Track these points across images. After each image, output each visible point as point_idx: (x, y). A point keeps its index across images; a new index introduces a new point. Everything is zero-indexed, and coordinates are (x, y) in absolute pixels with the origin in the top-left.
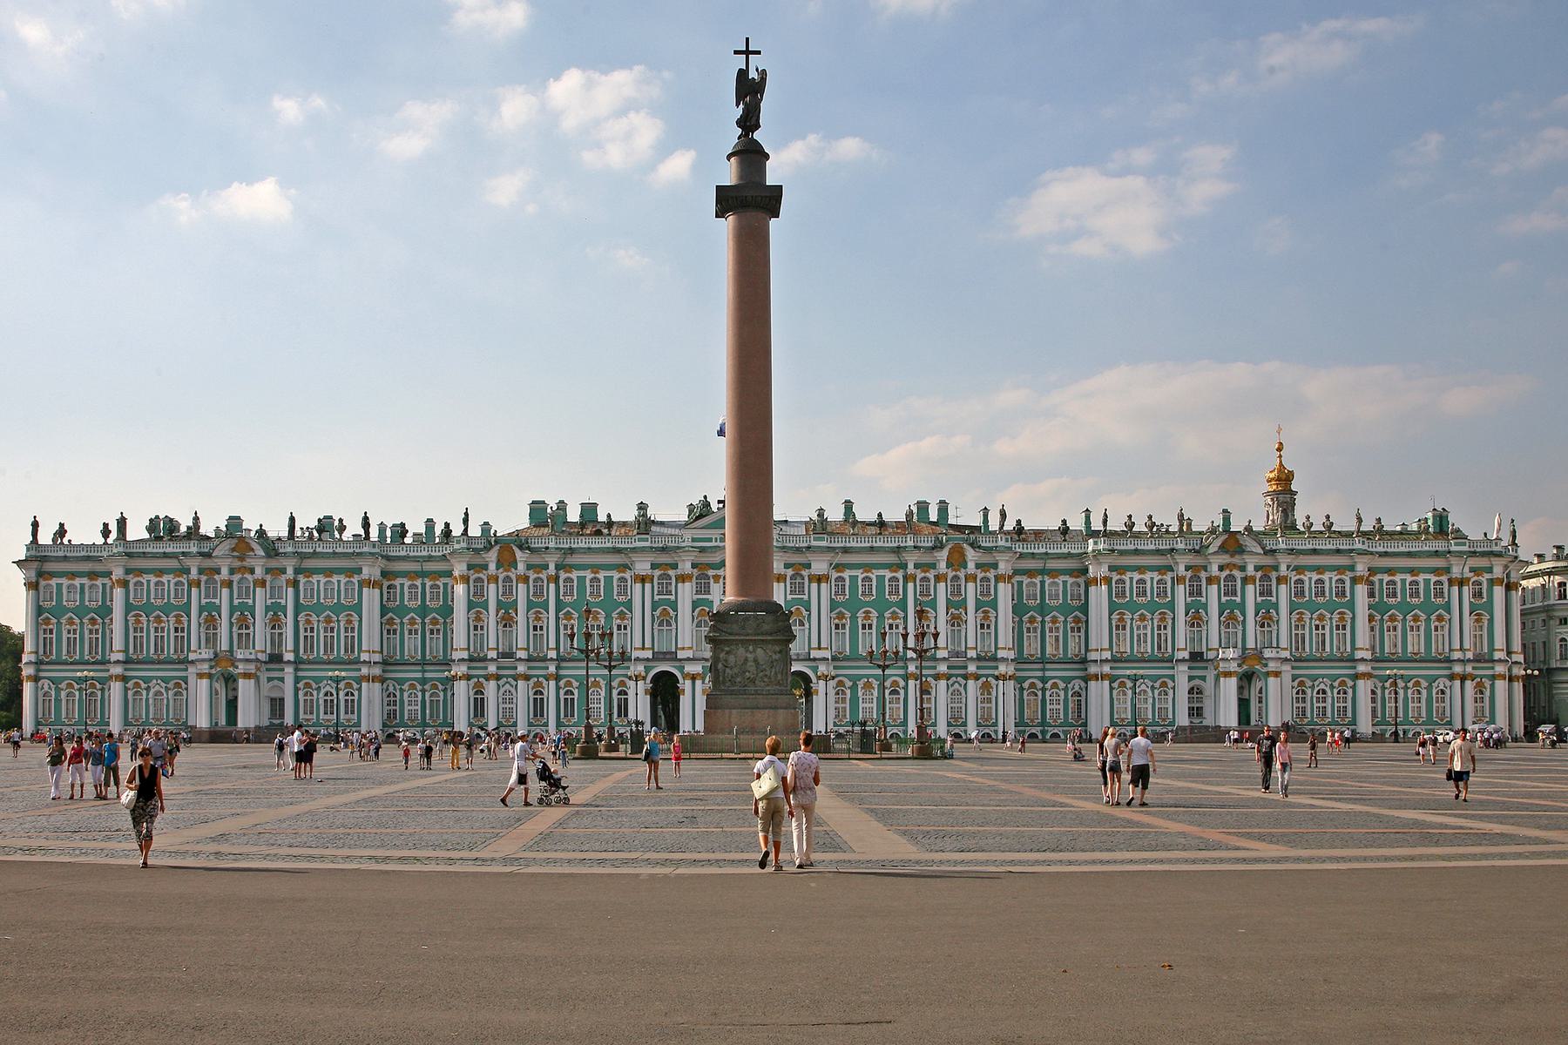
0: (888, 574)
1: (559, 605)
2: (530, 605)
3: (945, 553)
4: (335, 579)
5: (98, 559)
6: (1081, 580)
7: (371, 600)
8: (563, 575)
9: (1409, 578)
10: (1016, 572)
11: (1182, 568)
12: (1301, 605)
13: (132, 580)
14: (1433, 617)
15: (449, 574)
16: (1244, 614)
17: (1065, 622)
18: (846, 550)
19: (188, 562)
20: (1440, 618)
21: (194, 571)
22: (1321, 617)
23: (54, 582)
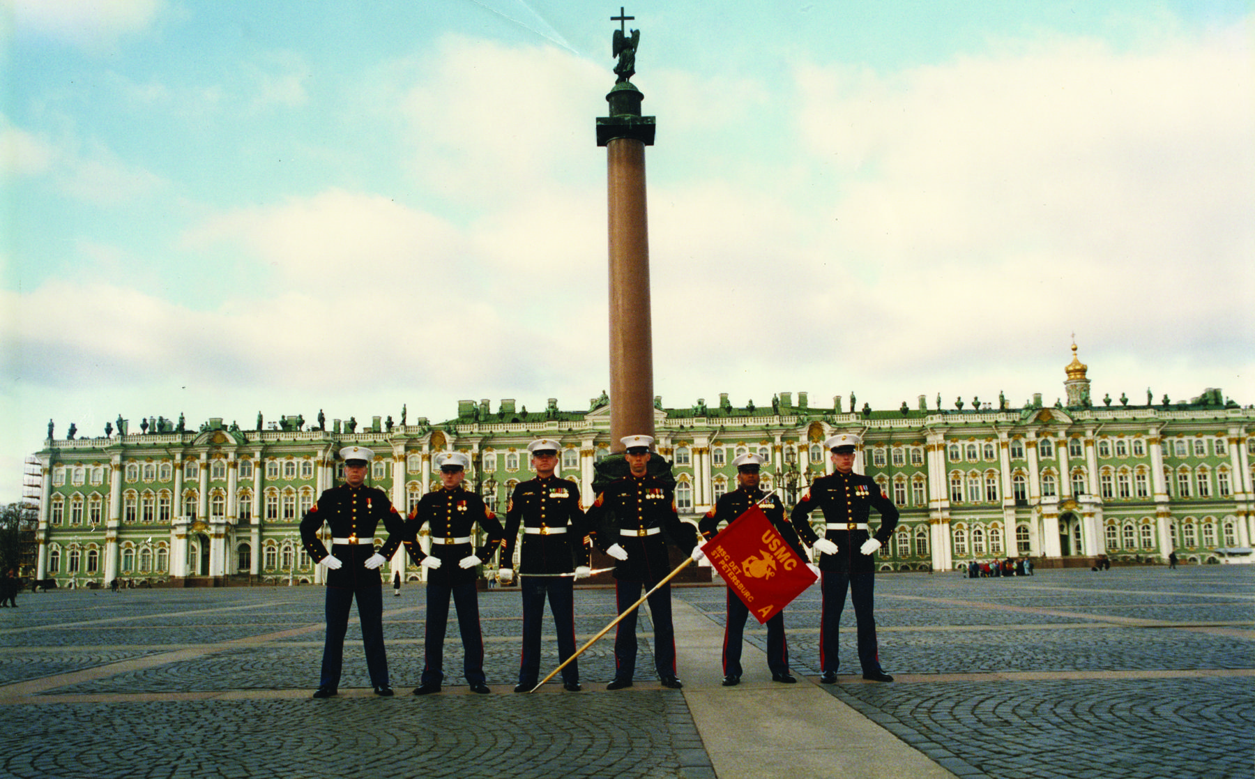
4: (294, 461)
6: (921, 448)
10: (866, 443)
14: (1217, 468)
15: (390, 455)
16: (1058, 470)
17: (909, 479)
19: (173, 451)
20: (1223, 469)
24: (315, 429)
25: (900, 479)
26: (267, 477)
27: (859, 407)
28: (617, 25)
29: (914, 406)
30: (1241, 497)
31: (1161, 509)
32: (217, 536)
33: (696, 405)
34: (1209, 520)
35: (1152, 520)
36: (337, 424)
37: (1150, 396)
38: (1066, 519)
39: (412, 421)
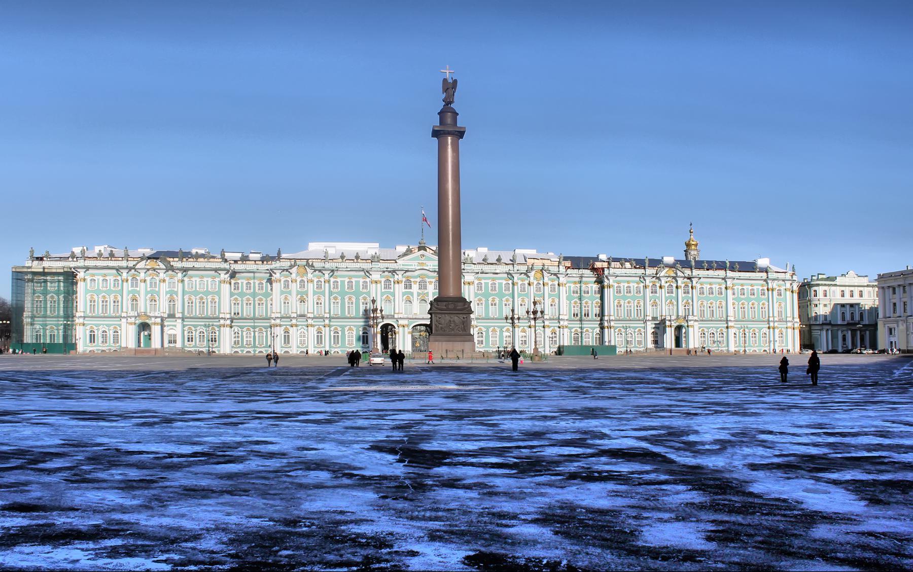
1: (331, 293)
2: (315, 293)
4: (205, 279)
8: (332, 280)
26: (186, 289)
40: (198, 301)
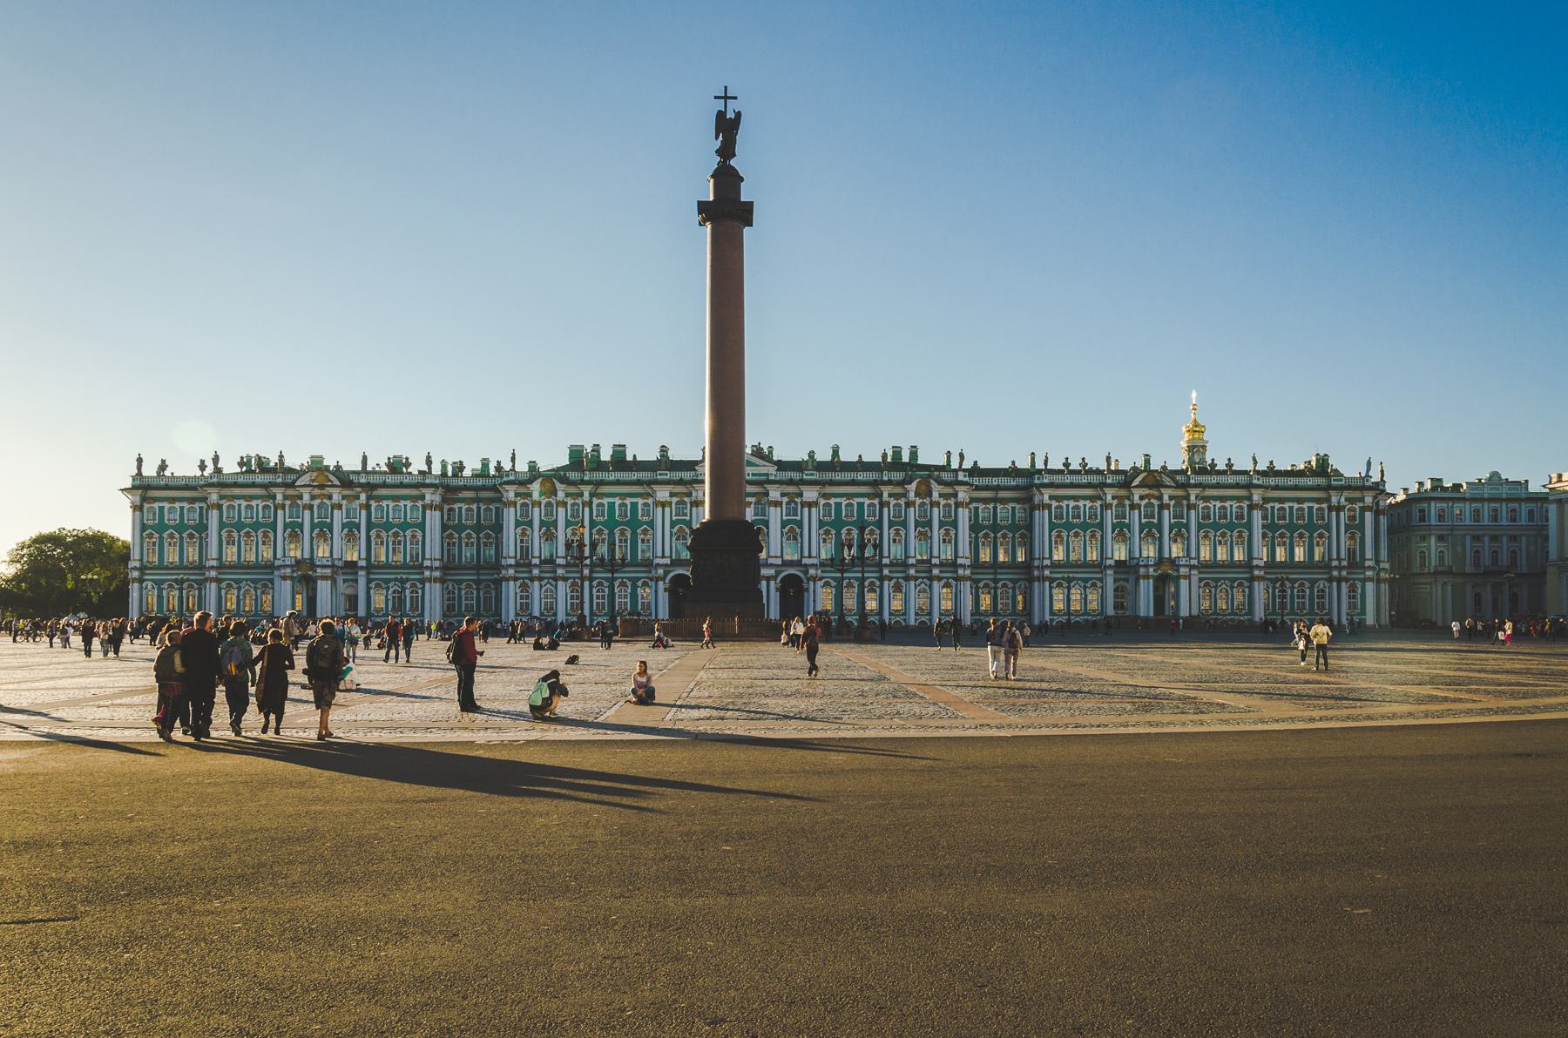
0: (867, 502)
3: (914, 485)
4: (402, 503)
5: (194, 488)
7: (433, 520)
8: (596, 501)
9: (1296, 506)
10: (972, 500)
11: (1109, 497)
12: (1207, 526)
13: (225, 504)
15: (499, 500)
16: (1160, 531)
18: (832, 483)
19: (274, 490)
21: (279, 497)
22: (1223, 535)
23: (156, 505)
24: (421, 472)
25: (1004, 536)
27: (967, 465)
28: (720, 105)
29: (1024, 464)
30: (1335, 563)
31: (1256, 572)
32: (324, 578)
33: (806, 458)
34: (1302, 585)
35: (1246, 584)
36: (444, 465)
37: (1255, 462)
38: (1162, 581)
39: (522, 467)
40: (391, 539)
